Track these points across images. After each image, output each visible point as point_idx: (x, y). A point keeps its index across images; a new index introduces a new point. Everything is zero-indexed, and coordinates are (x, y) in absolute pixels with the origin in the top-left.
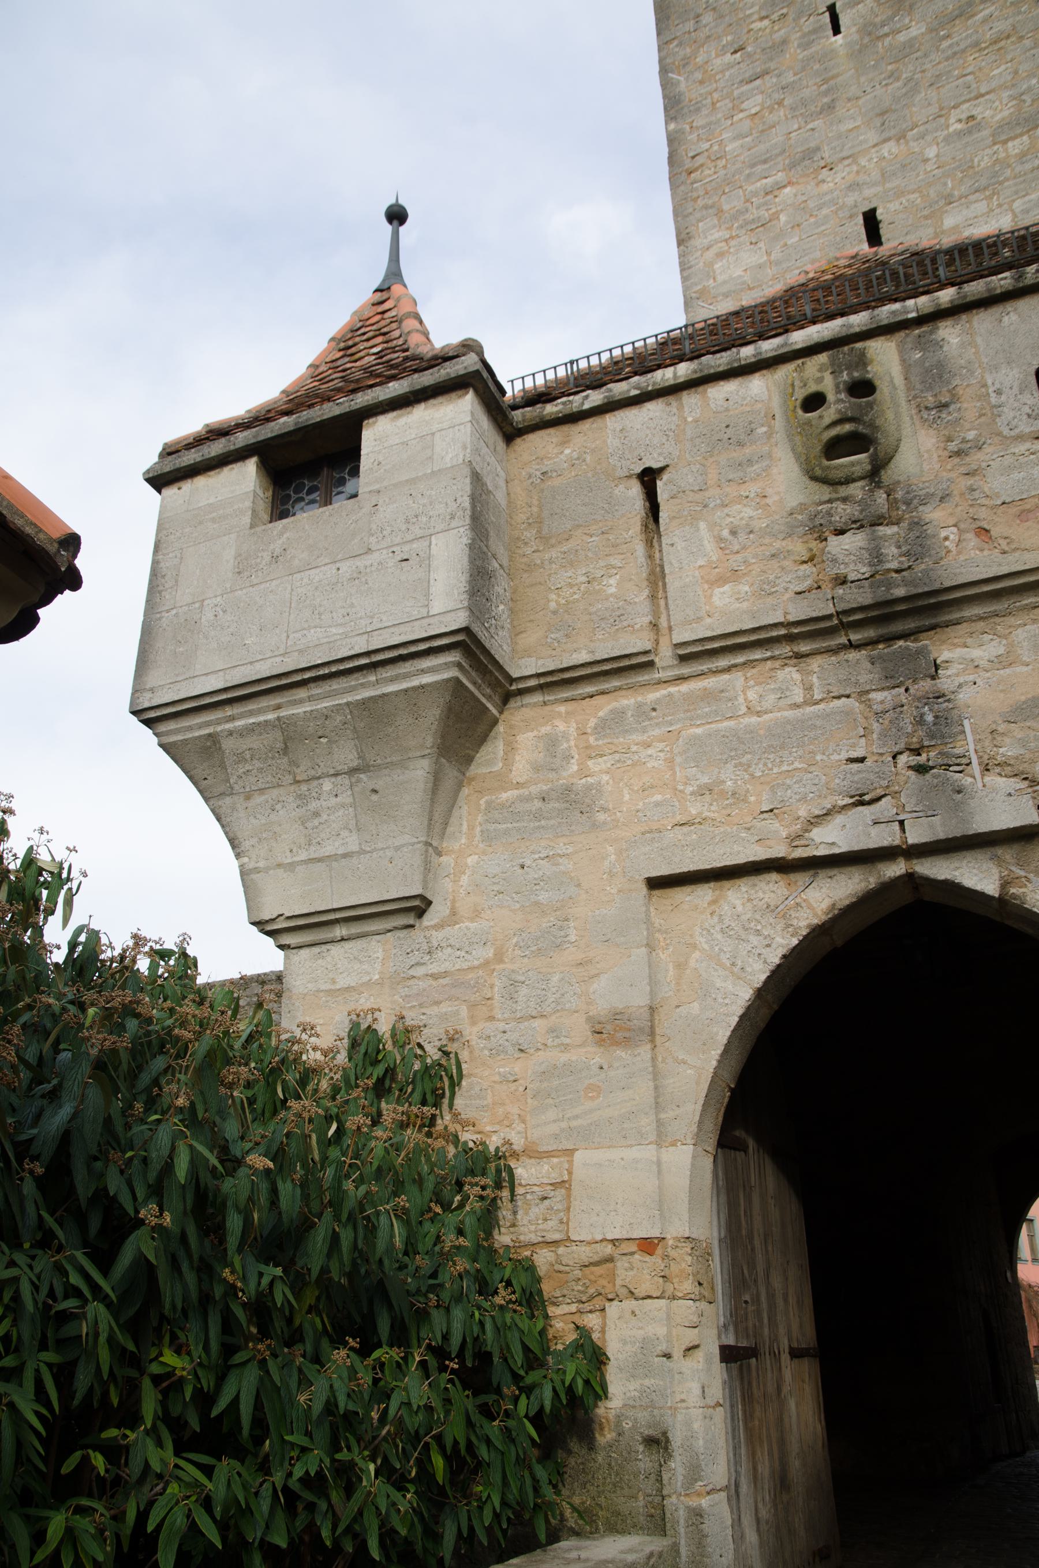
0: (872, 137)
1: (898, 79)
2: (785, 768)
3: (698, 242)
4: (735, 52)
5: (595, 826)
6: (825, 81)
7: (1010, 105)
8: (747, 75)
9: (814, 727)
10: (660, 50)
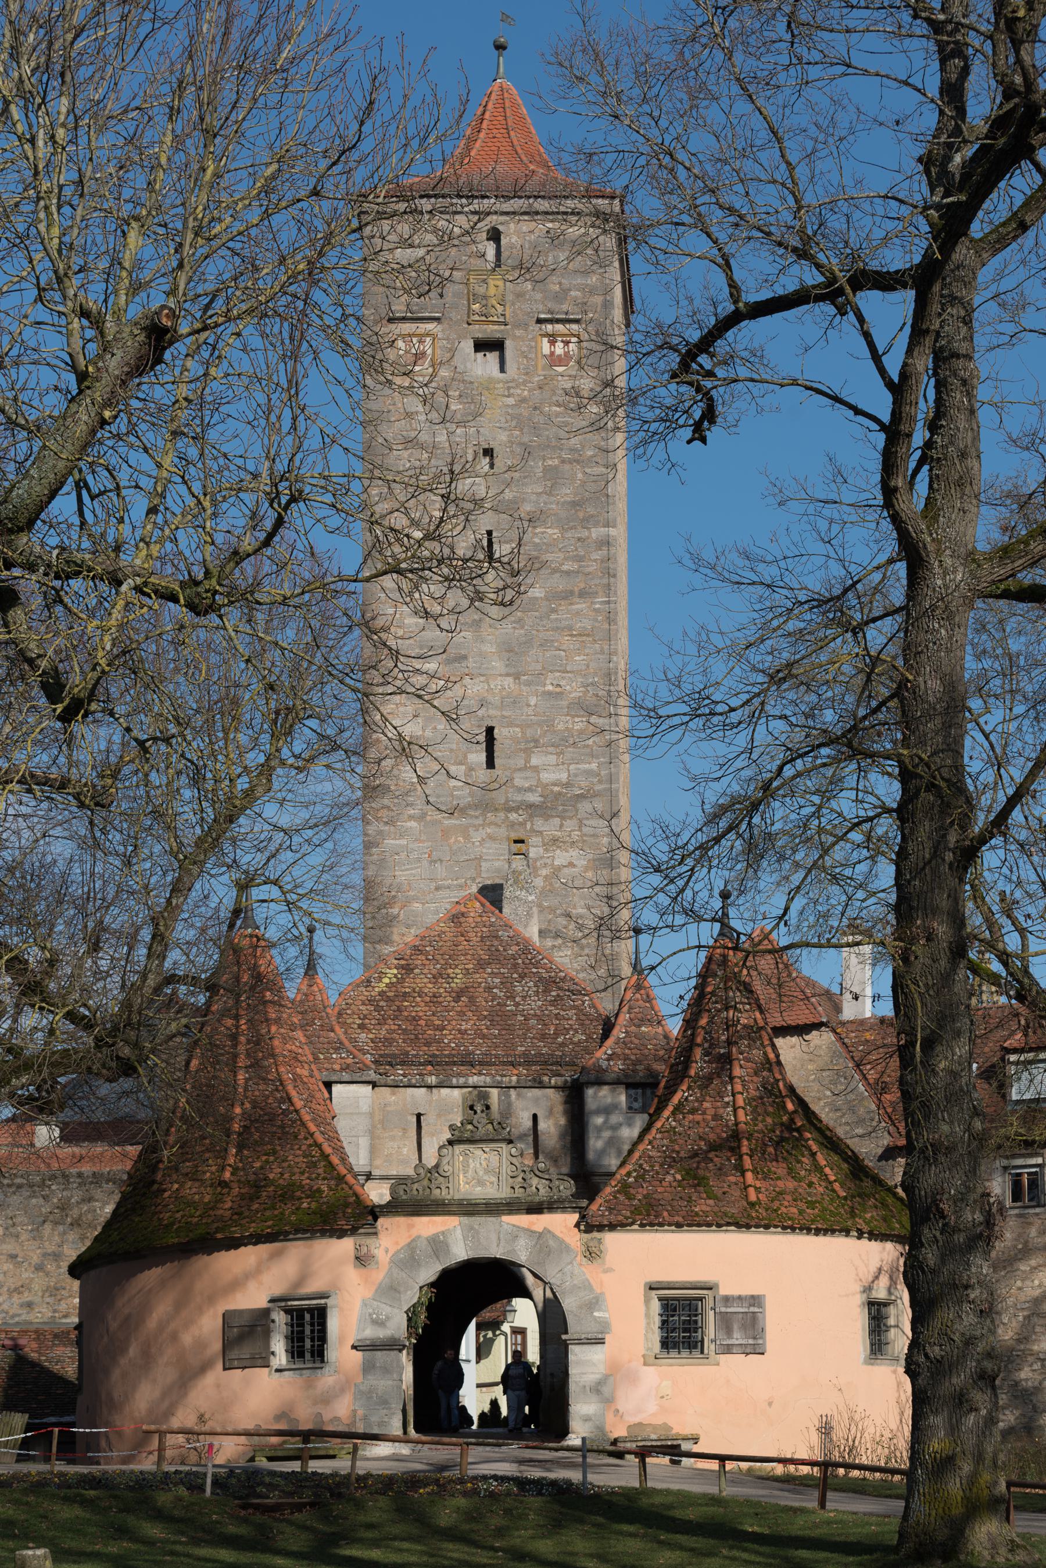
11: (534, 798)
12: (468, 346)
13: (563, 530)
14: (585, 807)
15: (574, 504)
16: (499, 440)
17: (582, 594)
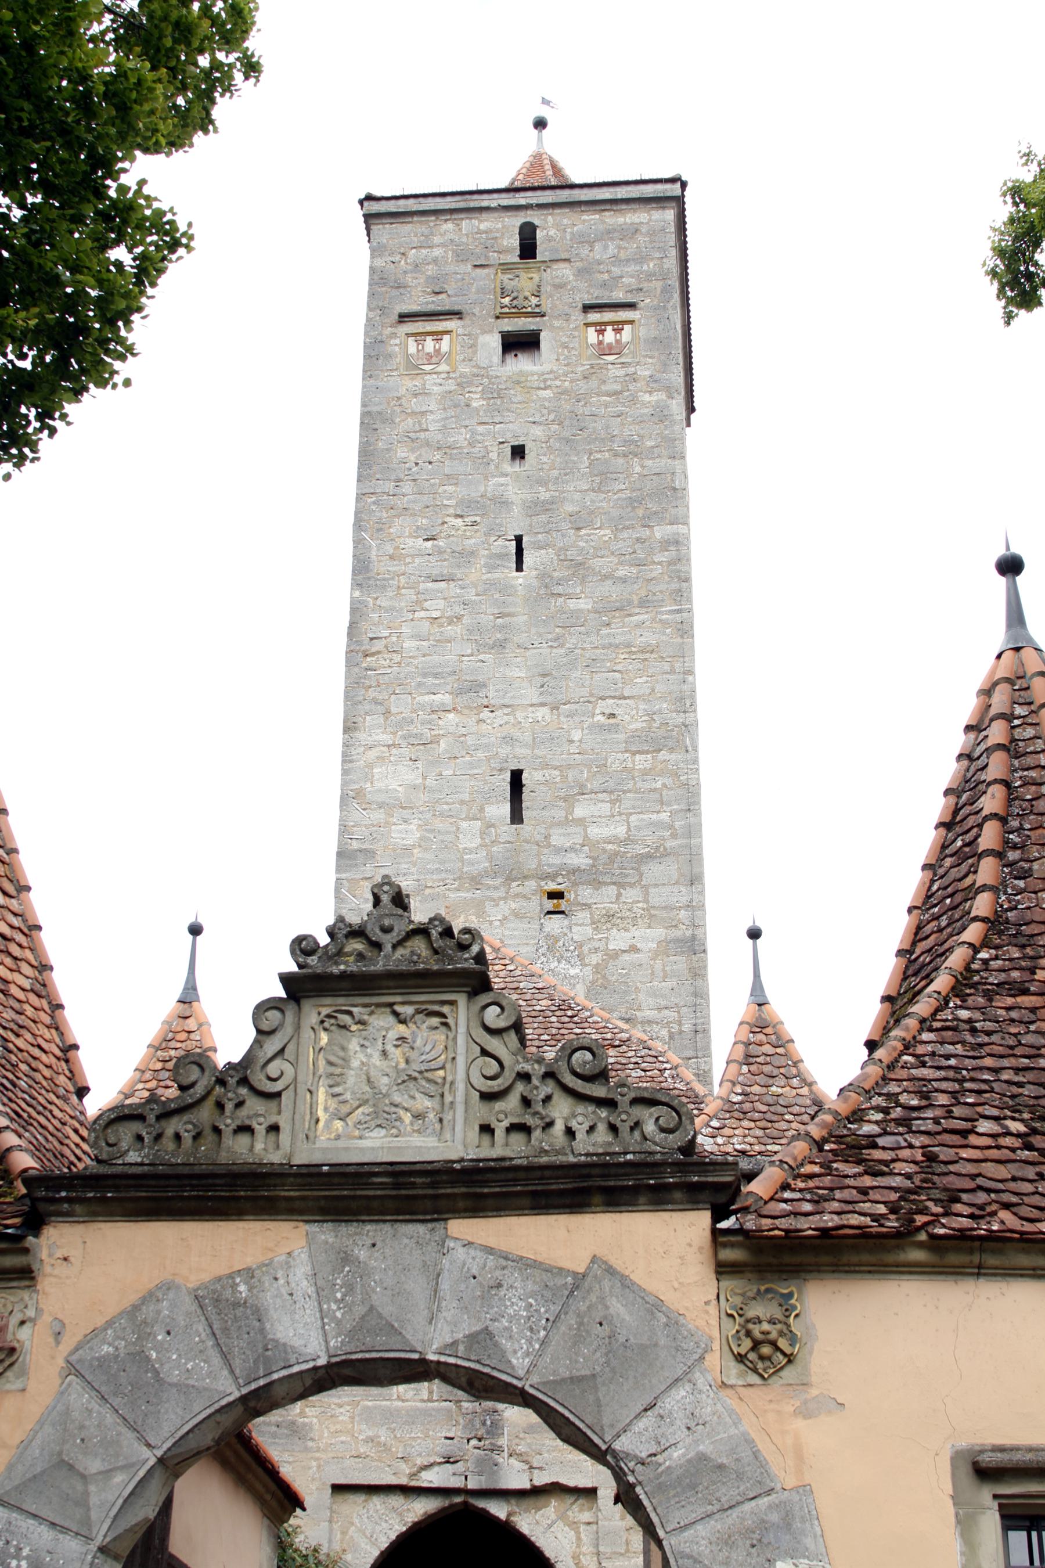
0: (531, 694)
1: (562, 646)
2: (413, 1435)
3: (361, 736)
4: (428, 540)
5: (307, 1449)
6: (502, 615)
7: (644, 718)
8: (435, 572)
9: (431, 1415)
10: (358, 499)
11: (580, 860)
12: (495, 342)
13: (616, 530)
14: (653, 871)
15: (633, 503)
16: (532, 437)
17: (643, 603)
